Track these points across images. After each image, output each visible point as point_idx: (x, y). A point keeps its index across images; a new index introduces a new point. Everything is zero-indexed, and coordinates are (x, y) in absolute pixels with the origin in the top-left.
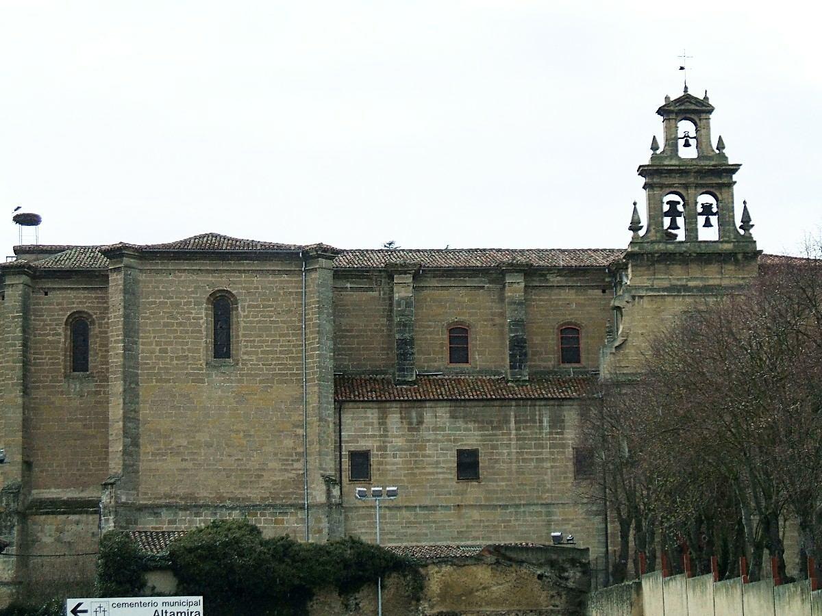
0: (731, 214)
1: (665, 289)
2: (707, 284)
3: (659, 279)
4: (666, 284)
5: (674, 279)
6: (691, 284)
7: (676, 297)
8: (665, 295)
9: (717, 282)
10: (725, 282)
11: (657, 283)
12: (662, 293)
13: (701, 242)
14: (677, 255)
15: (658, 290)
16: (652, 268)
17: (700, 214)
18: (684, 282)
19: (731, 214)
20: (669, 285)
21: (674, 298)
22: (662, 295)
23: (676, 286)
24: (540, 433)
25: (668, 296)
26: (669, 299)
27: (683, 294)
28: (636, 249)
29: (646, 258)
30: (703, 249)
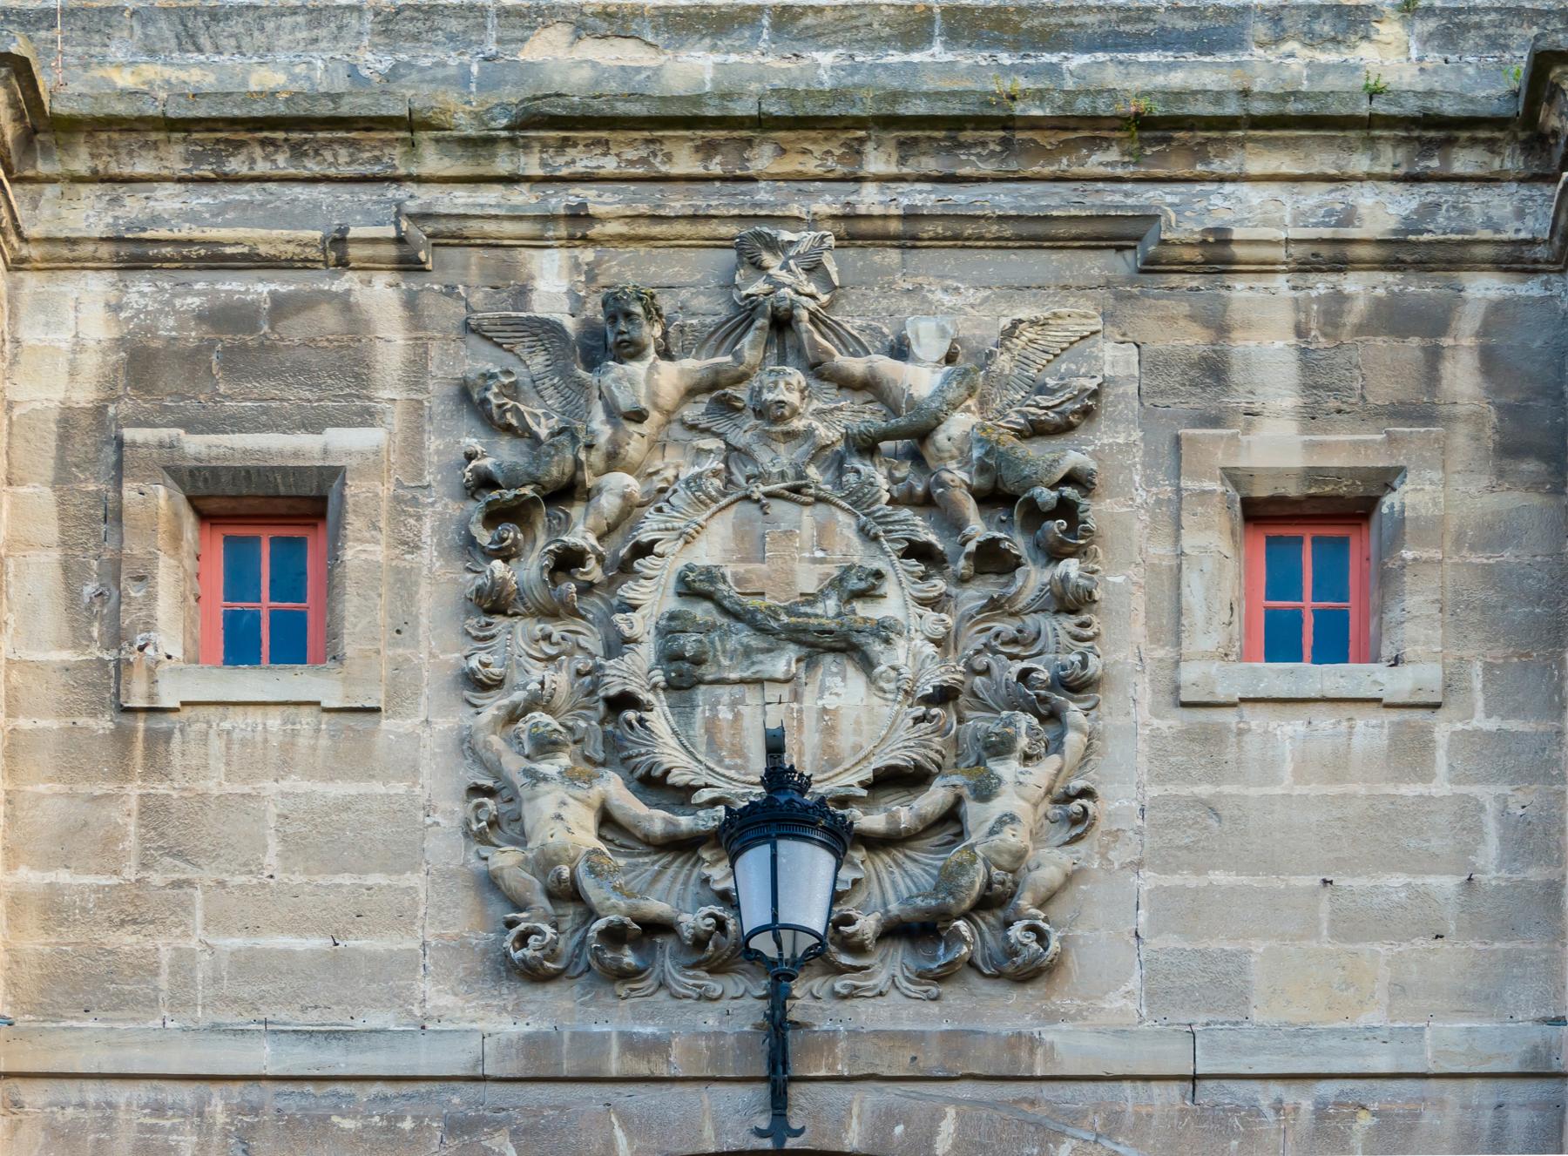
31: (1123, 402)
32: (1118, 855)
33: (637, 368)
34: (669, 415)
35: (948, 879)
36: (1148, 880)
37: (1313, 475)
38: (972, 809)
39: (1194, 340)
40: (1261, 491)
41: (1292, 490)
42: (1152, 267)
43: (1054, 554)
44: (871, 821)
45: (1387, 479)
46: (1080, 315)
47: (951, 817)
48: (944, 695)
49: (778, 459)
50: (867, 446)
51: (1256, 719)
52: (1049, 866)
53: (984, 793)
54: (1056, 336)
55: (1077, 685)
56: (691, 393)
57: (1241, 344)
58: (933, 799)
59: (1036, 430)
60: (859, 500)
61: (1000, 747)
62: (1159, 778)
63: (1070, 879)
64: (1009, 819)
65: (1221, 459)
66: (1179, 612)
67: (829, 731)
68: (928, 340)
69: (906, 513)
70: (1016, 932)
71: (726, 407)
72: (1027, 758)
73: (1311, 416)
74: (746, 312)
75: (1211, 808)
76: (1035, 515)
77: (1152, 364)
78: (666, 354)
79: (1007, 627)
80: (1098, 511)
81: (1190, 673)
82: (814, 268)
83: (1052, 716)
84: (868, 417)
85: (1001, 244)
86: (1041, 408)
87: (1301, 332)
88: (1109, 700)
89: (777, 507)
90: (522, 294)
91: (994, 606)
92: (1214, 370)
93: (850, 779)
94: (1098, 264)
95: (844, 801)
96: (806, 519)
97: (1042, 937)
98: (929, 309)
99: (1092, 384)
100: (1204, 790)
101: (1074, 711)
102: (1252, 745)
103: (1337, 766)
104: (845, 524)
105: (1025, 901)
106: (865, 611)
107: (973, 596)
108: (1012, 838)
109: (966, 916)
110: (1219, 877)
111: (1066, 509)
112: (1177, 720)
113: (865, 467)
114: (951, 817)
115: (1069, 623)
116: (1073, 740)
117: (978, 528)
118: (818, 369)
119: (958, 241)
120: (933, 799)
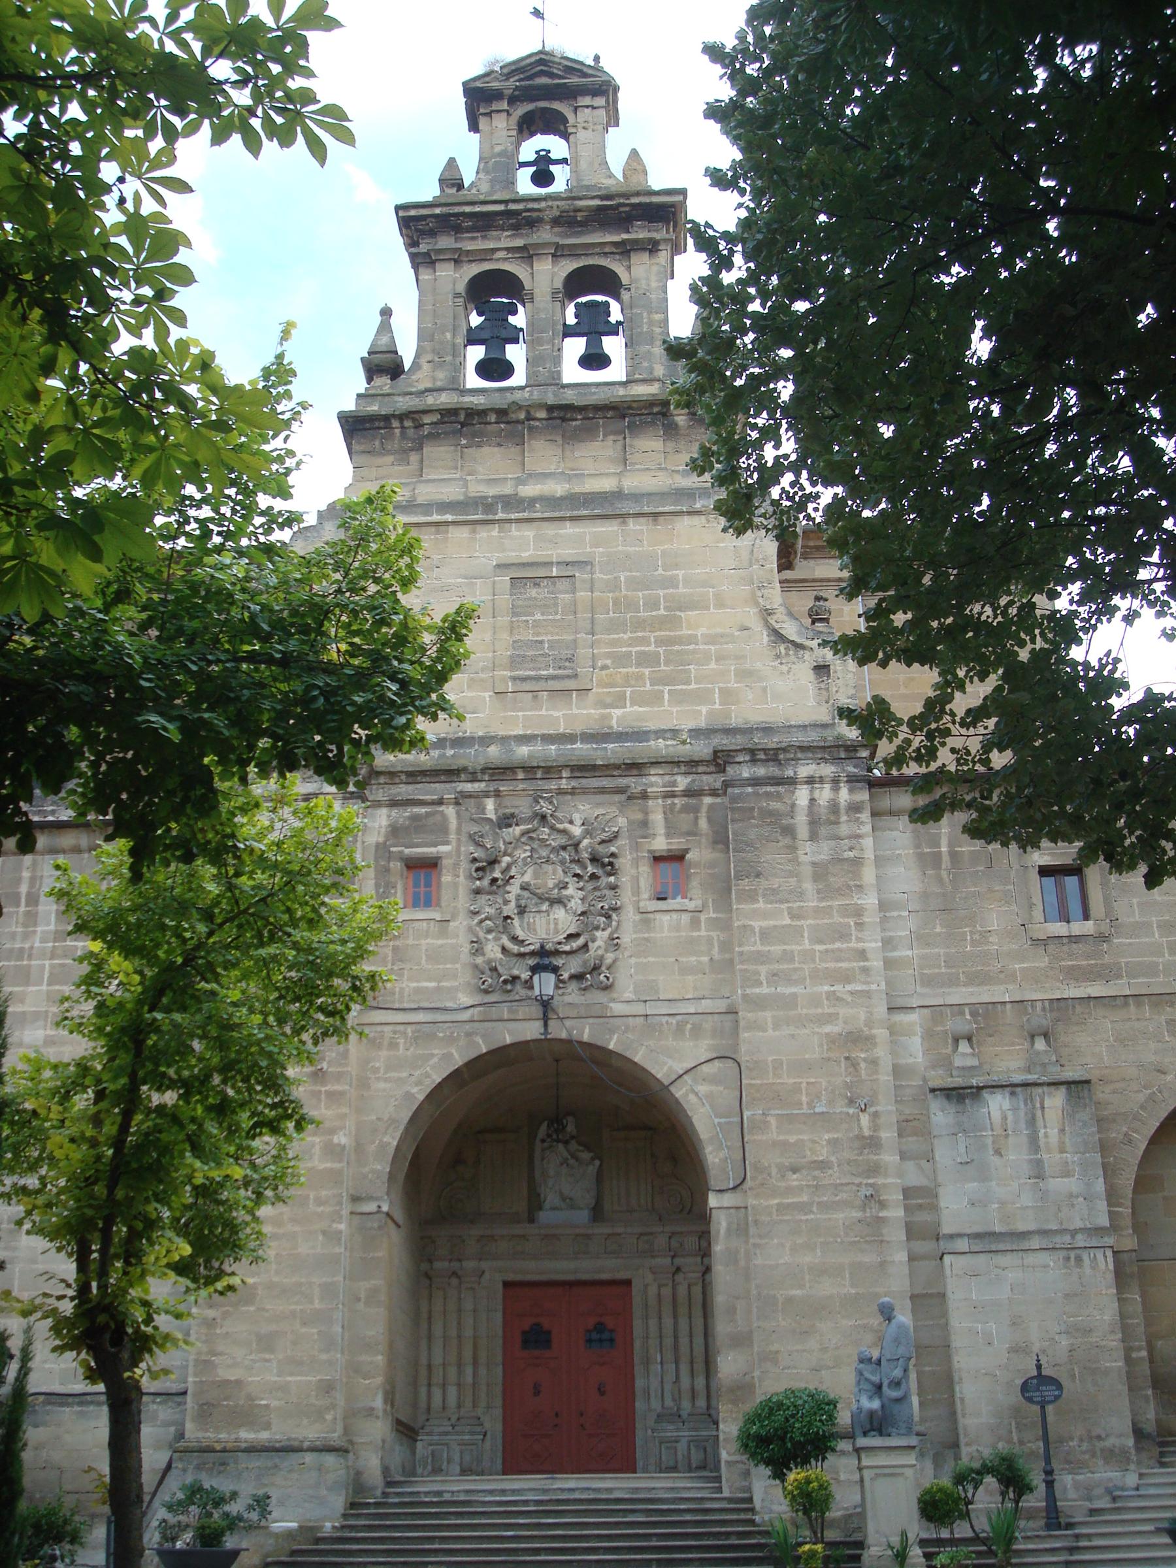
0: (658, 317)
1: (444, 507)
2: (577, 489)
3: (434, 481)
4: (452, 492)
5: (479, 481)
6: (529, 490)
7: (478, 527)
8: (447, 523)
9: (606, 485)
10: (631, 483)
11: (426, 493)
12: (436, 518)
13: (569, 386)
14: (493, 418)
15: (427, 508)
16: (414, 457)
17: (569, 332)
18: (507, 490)
19: (658, 317)
20: (462, 498)
21: (474, 531)
22: (437, 524)
23: (486, 498)
24: (26, 936)
25: (454, 523)
26: (462, 533)
27: (500, 515)
28: (374, 408)
29: (397, 431)
30: (570, 397)
31: (624, 833)
32: (626, 954)
33: (511, 830)
34: (518, 840)
35: (585, 962)
36: (633, 960)
37: (669, 850)
38: (590, 944)
39: (639, 816)
40: (657, 854)
41: (665, 854)
42: (629, 798)
43: (610, 875)
44: (567, 948)
45: (687, 851)
46: (613, 810)
47: (585, 946)
48: (583, 913)
49: (544, 853)
50: (564, 848)
51: (658, 916)
52: (609, 958)
53: (593, 941)
54: (608, 817)
55: (615, 909)
56: (523, 834)
57: (652, 817)
58: (581, 941)
59: (603, 842)
60: (563, 862)
61: (597, 928)
62: (635, 932)
63: (615, 961)
64: (599, 947)
65: (647, 847)
66: (638, 887)
67: (556, 924)
68: (578, 822)
69: (573, 866)
70: (602, 977)
71: (531, 838)
72: (603, 930)
73: (668, 835)
74: (536, 815)
75: (647, 940)
76: (603, 865)
77: (631, 823)
78: (517, 825)
79: (597, 893)
80: (618, 863)
81: (642, 904)
82: (551, 803)
83: (608, 917)
84: (562, 840)
85: (594, 793)
86: (604, 836)
87: (665, 813)
88: (623, 912)
89: (544, 865)
90: (483, 811)
91: (596, 889)
92: (645, 824)
93: (561, 937)
94: (617, 798)
95: (560, 943)
96: (549, 868)
97: (608, 978)
98: (578, 811)
99: (616, 829)
100: (646, 935)
101: (614, 916)
102: (657, 923)
103: (677, 928)
104: (559, 869)
105: (603, 968)
106: (565, 892)
107: (590, 886)
108: (600, 952)
109: (590, 973)
110: (651, 959)
111: (611, 864)
112: (638, 917)
113: (562, 853)
114: (585, 946)
115: (612, 892)
116: (614, 923)
117: (591, 869)
118: (552, 828)
119: (584, 793)
120: (581, 941)
